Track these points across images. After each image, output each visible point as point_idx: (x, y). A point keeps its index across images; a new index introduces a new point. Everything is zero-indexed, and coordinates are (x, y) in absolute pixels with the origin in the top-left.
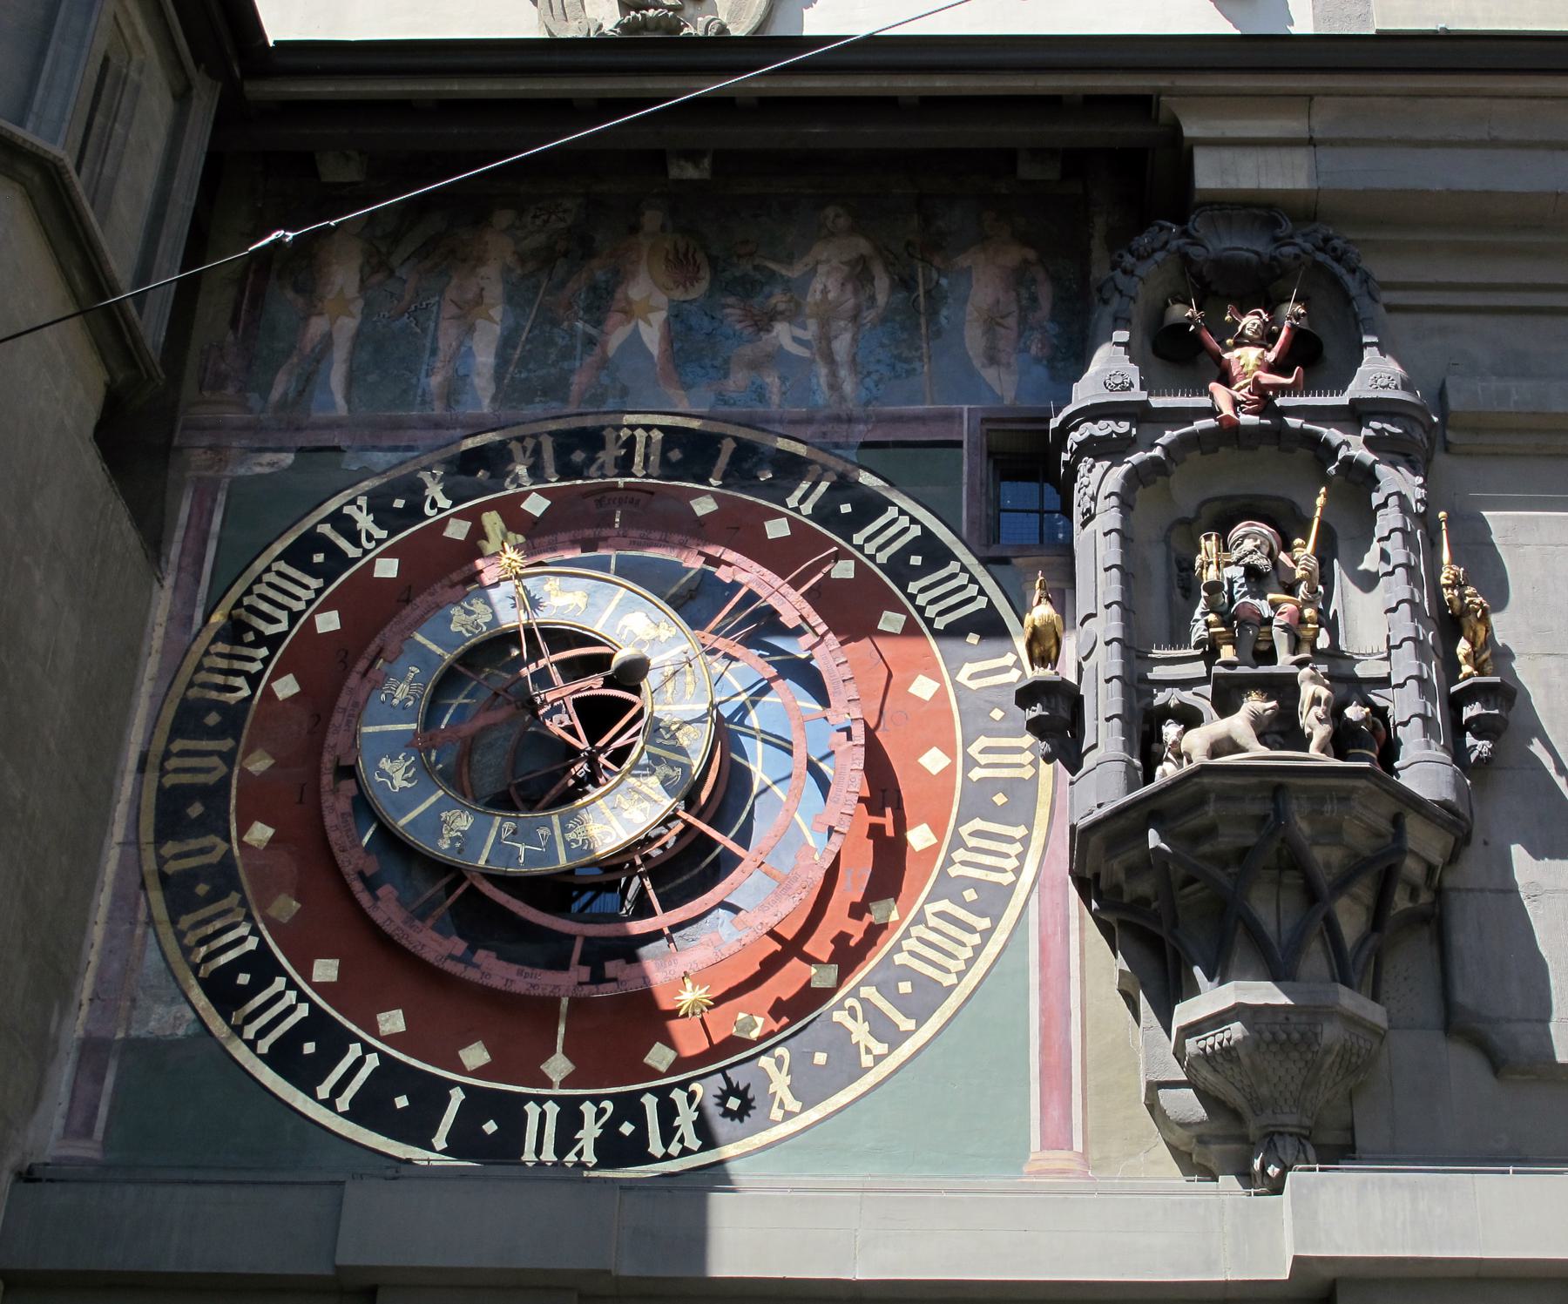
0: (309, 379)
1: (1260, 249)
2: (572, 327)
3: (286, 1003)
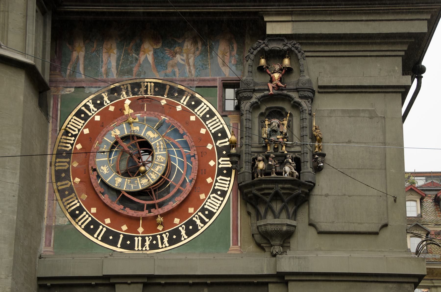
0: (75, 70)
1: (280, 47)
2: (132, 55)
3: (86, 217)
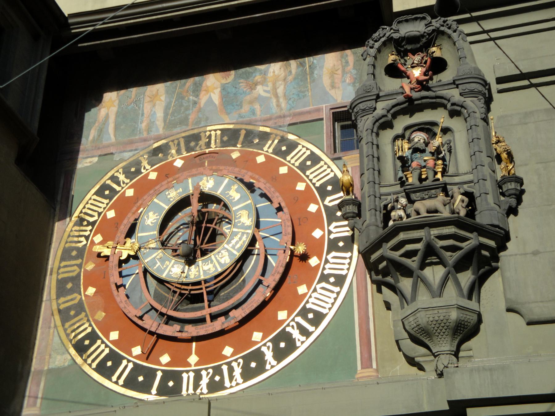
0: (101, 131)
1: (419, 30)
2: (189, 99)
3: (100, 349)
